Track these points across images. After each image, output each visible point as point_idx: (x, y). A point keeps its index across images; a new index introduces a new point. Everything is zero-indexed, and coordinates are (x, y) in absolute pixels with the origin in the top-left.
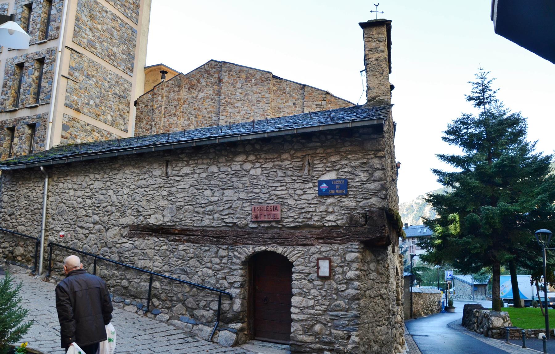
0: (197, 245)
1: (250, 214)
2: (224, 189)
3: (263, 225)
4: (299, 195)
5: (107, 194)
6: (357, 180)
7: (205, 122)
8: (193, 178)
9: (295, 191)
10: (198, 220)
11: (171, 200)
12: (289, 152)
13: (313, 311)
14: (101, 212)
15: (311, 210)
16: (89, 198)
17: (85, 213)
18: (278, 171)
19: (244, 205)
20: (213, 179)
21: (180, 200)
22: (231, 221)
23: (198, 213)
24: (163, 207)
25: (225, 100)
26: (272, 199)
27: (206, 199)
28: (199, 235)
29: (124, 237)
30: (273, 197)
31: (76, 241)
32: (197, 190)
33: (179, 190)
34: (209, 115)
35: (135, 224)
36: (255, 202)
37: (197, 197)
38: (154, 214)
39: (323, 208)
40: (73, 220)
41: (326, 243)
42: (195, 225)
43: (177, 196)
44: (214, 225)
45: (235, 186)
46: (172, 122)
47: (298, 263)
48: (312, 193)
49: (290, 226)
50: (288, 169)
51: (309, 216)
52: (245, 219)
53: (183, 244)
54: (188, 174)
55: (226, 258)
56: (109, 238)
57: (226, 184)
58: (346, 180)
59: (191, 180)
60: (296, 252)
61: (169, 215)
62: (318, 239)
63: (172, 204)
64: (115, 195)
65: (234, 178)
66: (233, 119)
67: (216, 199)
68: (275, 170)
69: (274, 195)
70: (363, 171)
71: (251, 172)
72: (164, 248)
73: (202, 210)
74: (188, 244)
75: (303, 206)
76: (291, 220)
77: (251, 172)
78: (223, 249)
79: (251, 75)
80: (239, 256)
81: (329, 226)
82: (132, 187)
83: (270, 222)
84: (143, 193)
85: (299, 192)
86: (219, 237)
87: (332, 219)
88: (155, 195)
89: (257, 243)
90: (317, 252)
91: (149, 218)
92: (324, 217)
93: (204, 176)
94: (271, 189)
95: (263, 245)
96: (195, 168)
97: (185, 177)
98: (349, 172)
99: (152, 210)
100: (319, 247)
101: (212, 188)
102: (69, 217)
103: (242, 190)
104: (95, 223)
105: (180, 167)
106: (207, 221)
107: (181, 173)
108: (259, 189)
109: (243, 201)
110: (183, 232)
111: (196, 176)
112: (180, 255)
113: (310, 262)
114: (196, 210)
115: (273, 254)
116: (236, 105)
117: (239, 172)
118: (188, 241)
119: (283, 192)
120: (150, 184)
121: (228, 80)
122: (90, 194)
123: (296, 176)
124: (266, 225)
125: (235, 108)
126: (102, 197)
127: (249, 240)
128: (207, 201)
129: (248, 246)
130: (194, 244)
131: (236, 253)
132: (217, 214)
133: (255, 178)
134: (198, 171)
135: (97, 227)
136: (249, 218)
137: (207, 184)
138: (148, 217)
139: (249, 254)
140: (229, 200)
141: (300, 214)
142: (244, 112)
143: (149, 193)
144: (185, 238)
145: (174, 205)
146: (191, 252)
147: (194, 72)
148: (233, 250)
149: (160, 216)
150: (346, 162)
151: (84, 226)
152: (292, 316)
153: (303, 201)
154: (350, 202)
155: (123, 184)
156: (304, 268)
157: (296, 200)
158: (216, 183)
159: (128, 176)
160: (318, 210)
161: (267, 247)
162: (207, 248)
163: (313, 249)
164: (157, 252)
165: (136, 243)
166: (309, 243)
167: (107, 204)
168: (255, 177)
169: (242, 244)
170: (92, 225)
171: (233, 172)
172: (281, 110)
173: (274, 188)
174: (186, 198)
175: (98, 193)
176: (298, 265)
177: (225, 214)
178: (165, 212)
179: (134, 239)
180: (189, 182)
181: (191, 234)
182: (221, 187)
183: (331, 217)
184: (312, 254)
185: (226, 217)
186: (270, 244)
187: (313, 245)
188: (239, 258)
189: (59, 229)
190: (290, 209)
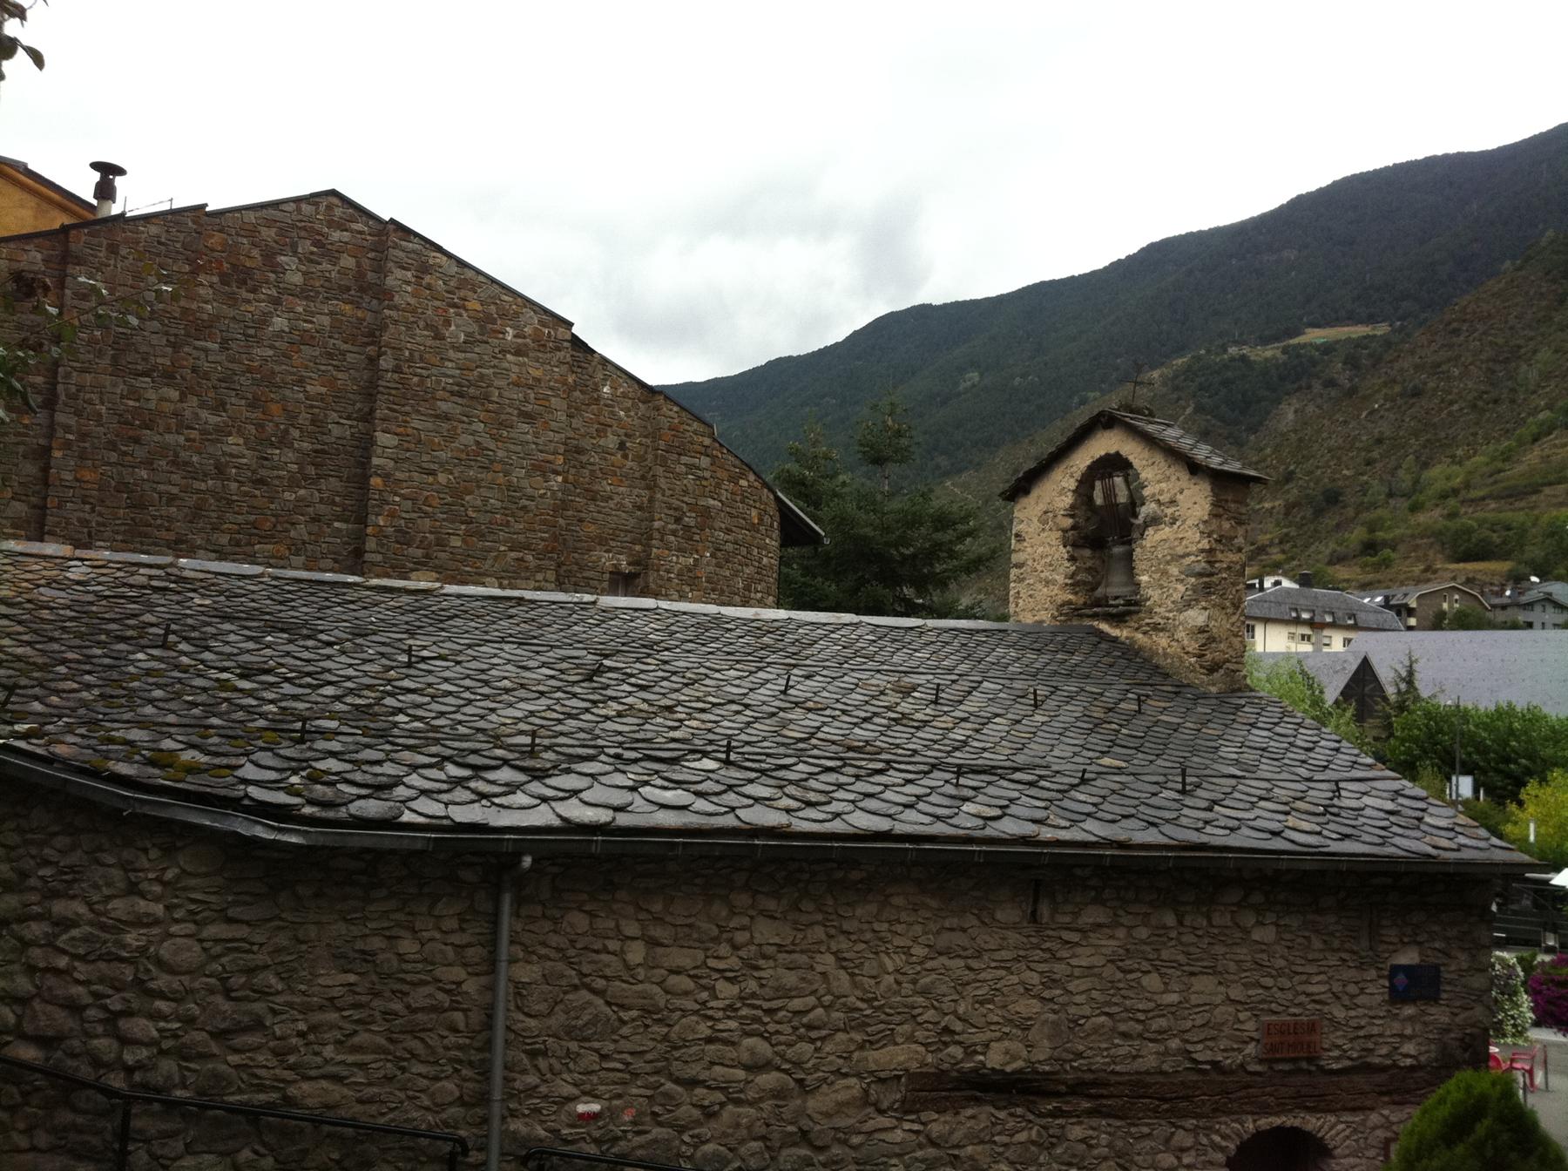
0: (1119, 1123)
1: (1252, 1039)
2: (1192, 974)
3: (1280, 1067)
4: (1353, 997)
5: (812, 967)
6: (1453, 968)
9: (1344, 986)
10: (1125, 1057)
11: (1051, 1000)
14: (786, 1029)
15: (1375, 1030)
16: (728, 979)
17: (708, 1032)
18: (1313, 937)
19: (1242, 1016)
20: (1165, 943)
21: (1079, 999)
22: (1209, 1059)
23: (1125, 1035)
24: (1030, 1019)
26: (1300, 1004)
27: (1150, 1000)
28: (1127, 1096)
29: (881, 1112)
30: (1302, 998)
31: (657, 1132)
32: (1124, 971)
33: (1077, 972)
36: (1262, 1010)
37: (1122, 992)
38: (999, 1040)
39: (1396, 1027)
40: (649, 1057)
41: (1395, 1103)
42: (1118, 1068)
43: (1071, 987)
44: (1165, 1067)
45: (1220, 968)
46: (152, 405)
47: (1347, 1152)
48: (1377, 991)
49: (1334, 1066)
50: (1332, 934)
51: (1371, 1046)
52: (1240, 1050)
53: (1080, 1123)
54: (1100, 926)
55: (1193, 1153)
57: (1197, 960)
58: (1436, 968)
60: (1341, 1126)
61: (1046, 1043)
62: (1381, 1094)
63: (1055, 1012)
64: (842, 972)
65: (1216, 947)
67: (1173, 998)
68: (1307, 934)
69: (1304, 993)
70: (1463, 949)
71: (1256, 936)
72: (1022, 1137)
73: (1139, 1028)
74: (1094, 1122)
75: (1363, 1023)
76: (1336, 1053)
77: (1256, 936)
78: (1185, 1130)
79: (503, 316)
80: (1224, 1144)
81: (1405, 1067)
82: (919, 951)
83: (1294, 1060)
84: (959, 972)
85: (1352, 989)
86: (1176, 1098)
87: (1413, 1052)
88: (1003, 982)
89: (1266, 1110)
90: (1382, 1126)
91: (984, 1054)
92: (1396, 1048)
93: (1144, 936)
94: (1297, 978)
95: (1277, 1114)
96: (1121, 912)
97: (1091, 935)
98: (1440, 951)
99: (993, 1028)
100: (1386, 1112)
101: (1163, 970)
102: (628, 1046)
103: (1236, 978)
104: (756, 1067)
106: (1149, 1061)
107: (1080, 921)
109: (1239, 1007)
110: (1079, 1088)
111: (1121, 933)
112: (1074, 1156)
113: (1369, 1147)
114: (1123, 1027)
115: (1295, 1131)
116: (444, 406)
117: (1227, 932)
119: (1323, 988)
120: (986, 947)
121: (412, 301)
122: (734, 962)
123: (1347, 951)
124: (1286, 1067)
125: (437, 416)
127: (1246, 1104)
128: (1151, 1005)
129: (1244, 1117)
130: (1111, 1121)
131: (1217, 1138)
132: (1177, 1041)
133: (1263, 951)
135: (768, 1079)
136: (1251, 1049)
137: (1151, 956)
138: (979, 1048)
139: (1246, 1137)
140: (1206, 1004)
141: (1351, 1040)
143: (983, 976)
144: (1086, 1105)
145: (1063, 1015)
146: (1104, 1143)
147: (251, 217)
148: (1209, 1130)
149: (1016, 1046)
150: (1436, 928)
153: (1361, 1011)
154: (1439, 1015)
155: (881, 939)
156: (1358, 1160)
157: (1347, 1008)
158: (1173, 958)
159: (904, 916)
160: (1388, 1033)
161: (1284, 1119)
162: (1146, 1130)
163: (1374, 1118)
164: (1001, 1149)
165: (936, 1129)
166: (1368, 1103)
167: (812, 1000)
168: (1264, 947)
169: (1229, 1113)
170: (741, 1074)
171: (1216, 931)
172: (584, 458)
173: (1304, 977)
174: (1095, 994)
175: (771, 963)
176: (1346, 1157)
177: (1195, 1039)
178: (1033, 1035)
179: (924, 1116)
180: (1104, 950)
181: (1105, 1092)
182: (1186, 968)
183: (1409, 1048)
184: (1374, 1128)
185: (1200, 1047)
186: (1290, 1111)
187: (1372, 1109)
188: (1222, 1149)
189: (568, 1090)
190: (1337, 1029)
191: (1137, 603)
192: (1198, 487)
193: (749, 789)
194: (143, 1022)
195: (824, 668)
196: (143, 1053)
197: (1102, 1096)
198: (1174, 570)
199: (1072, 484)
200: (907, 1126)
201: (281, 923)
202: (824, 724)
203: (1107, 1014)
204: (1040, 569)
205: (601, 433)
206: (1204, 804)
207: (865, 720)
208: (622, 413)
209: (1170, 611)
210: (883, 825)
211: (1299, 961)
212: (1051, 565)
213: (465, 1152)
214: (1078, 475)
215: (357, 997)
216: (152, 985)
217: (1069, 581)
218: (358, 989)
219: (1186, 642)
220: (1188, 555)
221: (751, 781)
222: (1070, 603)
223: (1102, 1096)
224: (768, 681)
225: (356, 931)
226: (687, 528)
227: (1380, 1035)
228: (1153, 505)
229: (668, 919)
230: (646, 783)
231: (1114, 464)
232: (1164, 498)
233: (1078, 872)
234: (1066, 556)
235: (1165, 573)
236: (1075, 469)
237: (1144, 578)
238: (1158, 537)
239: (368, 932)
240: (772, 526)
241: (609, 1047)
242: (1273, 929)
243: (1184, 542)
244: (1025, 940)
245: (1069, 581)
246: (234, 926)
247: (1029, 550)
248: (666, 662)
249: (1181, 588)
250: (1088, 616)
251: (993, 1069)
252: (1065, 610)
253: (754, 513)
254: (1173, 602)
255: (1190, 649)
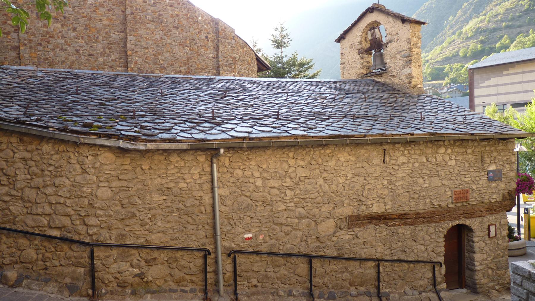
7: (101, 38)
8: (408, 167)
12: (471, 148)
13: (486, 262)
17: (285, 207)
18: (466, 163)
23: (413, 198)
24: (385, 195)
25: (132, 16)
27: (420, 186)
34: (107, 30)
35: (355, 214)
54: (404, 163)
56: (322, 233)
59: (407, 169)
62: (487, 211)
64: (326, 184)
66: (145, 43)
67: (427, 185)
68: (464, 162)
71: (449, 164)
80: (443, 231)
87: (495, 197)
89: (454, 219)
91: (372, 207)
93: (417, 166)
99: (374, 199)
100: (488, 217)
101: (424, 176)
104: (300, 218)
105: (397, 156)
107: (398, 162)
108: (454, 176)
111: (410, 165)
118: (406, 224)
126: (309, 187)
129: (448, 222)
131: (441, 229)
133: (451, 168)
134: (411, 161)
135: (305, 221)
137: (419, 172)
138: (370, 206)
139: (449, 228)
142: (158, 37)
151: (284, 222)
152: (477, 268)
162: (420, 228)
166: (483, 215)
171: (438, 163)
172: (195, 42)
179: (355, 230)
181: (408, 217)
183: (494, 196)
186: (461, 219)
188: (442, 232)
189: (241, 230)
191: (386, 70)
192: (405, 27)
193: (288, 125)
194: (93, 219)
195: (296, 93)
196: (95, 230)
197: (407, 219)
198: (398, 56)
199: (360, 33)
200: (349, 233)
201: (138, 180)
202: (303, 107)
203: (408, 192)
204: (351, 64)
205: (200, 33)
206: (430, 123)
207: (315, 106)
208: (206, 26)
209: (398, 70)
210: (337, 133)
211: (462, 171)
212: (354, 62)
213: (210, 254)
214: (362, 30)
215: (167, 204)
216: (96, 205)
217: (361, 66)
218: (167, 201)
219: (404, 80)
220: (403, 51)
221: (288, 123)
222: (362, 73)
223: (407, 219)
224: (280, 97)
225: (164, 181)
226: (230, 64)
227: (486, 193)
228: (390, 36)
229: (269, 170)
230: (255, 125)
231: (374, 26)
232: (394, 33)
233: (396, 145)
234: (360, 58)
235: (395, 57)
236: (361, 28)
237: (388, 61)
238: (392, 47)
239: (168, 181)
240: (255, 64)
241: (253, 215)
242: (454, 161)
243: (402, 47)
244: (382, 169)
245: (361, 66)
246: (122, 182)
247: (346, 58)
248: (245, 93)
249: (401, 62)
250: (369, 76)
251: (375, 212)
252: (361, 75)
253: (249, 59)
254: (399, 67)
255: (406, 82)
